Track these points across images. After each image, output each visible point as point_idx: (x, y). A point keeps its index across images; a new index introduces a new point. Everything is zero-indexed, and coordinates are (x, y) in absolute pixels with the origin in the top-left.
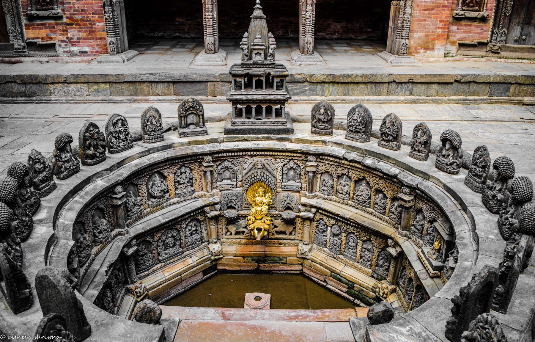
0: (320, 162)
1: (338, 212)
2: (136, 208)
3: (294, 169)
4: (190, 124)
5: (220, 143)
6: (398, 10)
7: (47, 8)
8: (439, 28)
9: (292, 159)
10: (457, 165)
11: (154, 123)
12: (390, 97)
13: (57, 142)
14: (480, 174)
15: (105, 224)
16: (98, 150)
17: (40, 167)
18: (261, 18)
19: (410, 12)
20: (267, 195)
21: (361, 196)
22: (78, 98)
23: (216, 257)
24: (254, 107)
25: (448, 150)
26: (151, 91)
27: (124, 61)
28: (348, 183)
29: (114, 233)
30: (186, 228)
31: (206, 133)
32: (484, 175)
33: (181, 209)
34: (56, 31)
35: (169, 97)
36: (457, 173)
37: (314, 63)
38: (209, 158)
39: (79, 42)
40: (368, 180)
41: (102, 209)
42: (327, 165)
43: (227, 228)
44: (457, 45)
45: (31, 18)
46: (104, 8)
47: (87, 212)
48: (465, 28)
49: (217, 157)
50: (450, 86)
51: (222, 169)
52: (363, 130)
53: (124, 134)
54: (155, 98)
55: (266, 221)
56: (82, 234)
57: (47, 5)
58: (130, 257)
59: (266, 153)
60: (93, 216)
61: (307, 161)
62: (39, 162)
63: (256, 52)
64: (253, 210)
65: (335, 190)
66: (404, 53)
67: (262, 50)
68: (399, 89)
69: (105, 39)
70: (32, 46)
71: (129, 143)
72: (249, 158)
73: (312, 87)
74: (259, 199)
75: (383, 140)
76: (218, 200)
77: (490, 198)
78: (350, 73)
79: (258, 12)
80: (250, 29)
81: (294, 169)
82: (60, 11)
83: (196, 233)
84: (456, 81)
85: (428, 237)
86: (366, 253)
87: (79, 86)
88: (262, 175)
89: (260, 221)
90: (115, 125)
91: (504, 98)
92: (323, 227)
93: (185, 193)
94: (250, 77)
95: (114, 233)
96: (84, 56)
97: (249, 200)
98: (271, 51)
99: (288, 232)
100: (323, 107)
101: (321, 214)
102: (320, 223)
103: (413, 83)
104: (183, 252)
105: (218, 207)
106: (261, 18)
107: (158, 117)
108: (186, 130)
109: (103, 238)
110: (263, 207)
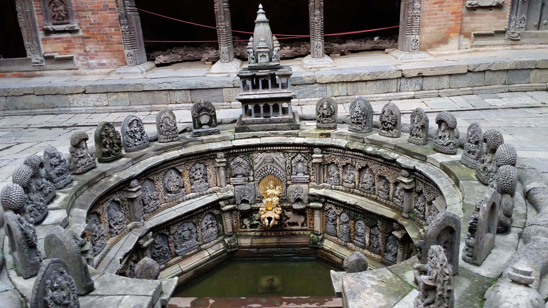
0: (326, 154)
1: (345, 200)
2: (152, 202)
3: (302, 162)
4: (204, 124)
5: (231, 140)
6: (407, 6)
7: (63, 22)
8: (451, 20)
9: (299, 152)
10: (454, 145)
11: (168, 124)
12: (400, 94)
13: (72, 140)
14: (474, 150)
15: (120, 216)
16: (114, 148)
17: (55, 161)
18: (264, 22)
19: (419, 7)
20: (277, 187)
21: (365, 183)
22: (98, 108)
23: (232, 250)
24: (261, 105)
25: (444, 131)
26: (169, 99)
27: (142, 73)
28: (353, 172)
29: (130, 225)
31: (218, 132)
32: (478, 151)
33: (197, 203)
34: (73, 45)
35: (187, 105)
36: (455, 154)
37: (324, 66)
39: (97, 55)
40: (370, 167)
41: (117, 203)
42: (332, 156)
43: (242, 222)
44: (472, 35)
45: (48, 32)
46: (120, 21)
47: (103, 204)
48: (480, 18)
49: (229, 154)
50: (463, 76)
52: (365, 121)
53: (139, 133)
54: (174, 106)
55: (277, 211)
56: (97, 225)
57: (63, 20)
58: (145, 249)
59: (274, 148)
60: (108, 208)
61: (313, 153)
62: (54, 157)
63: (261, 55)
64: (264, 201)
65: (341, 180)
66: (415, 49)
67: (266, 52)
68: (408, 83)
69: (123, 51)
70: (49, 59)
71: (144, 143)
73: (322, 88)
74: (269, 192)
75: (384, 129)
76: (231, 194)
77: (481, 170)
78: (358, 72)
79: (261, 17)
80: (254, 34)
81: (302, 162)
82: (76, 25)
83: (212, 226)
84: (469, 71)
85: (430, 217)
86: (374, 239)
87: (98, 96)
88: (272, 168)
89: (271, 212)
90: (130, 125)
91: (524, 85)
92: (332, 216)
94: (258, 77)
95: (130, 225)
96: (102, 68)
97: (262, 193)
98: (275, 53)
99: (300, 224)
100: (325, 103)
101: (330, 203)
102: (329, 213)
103: (423, 77)
104: (200, 246)
106: (264, 22)
107: (172, 118)
108: (200, 130)
109: (119, 230)
110: (274, 198)
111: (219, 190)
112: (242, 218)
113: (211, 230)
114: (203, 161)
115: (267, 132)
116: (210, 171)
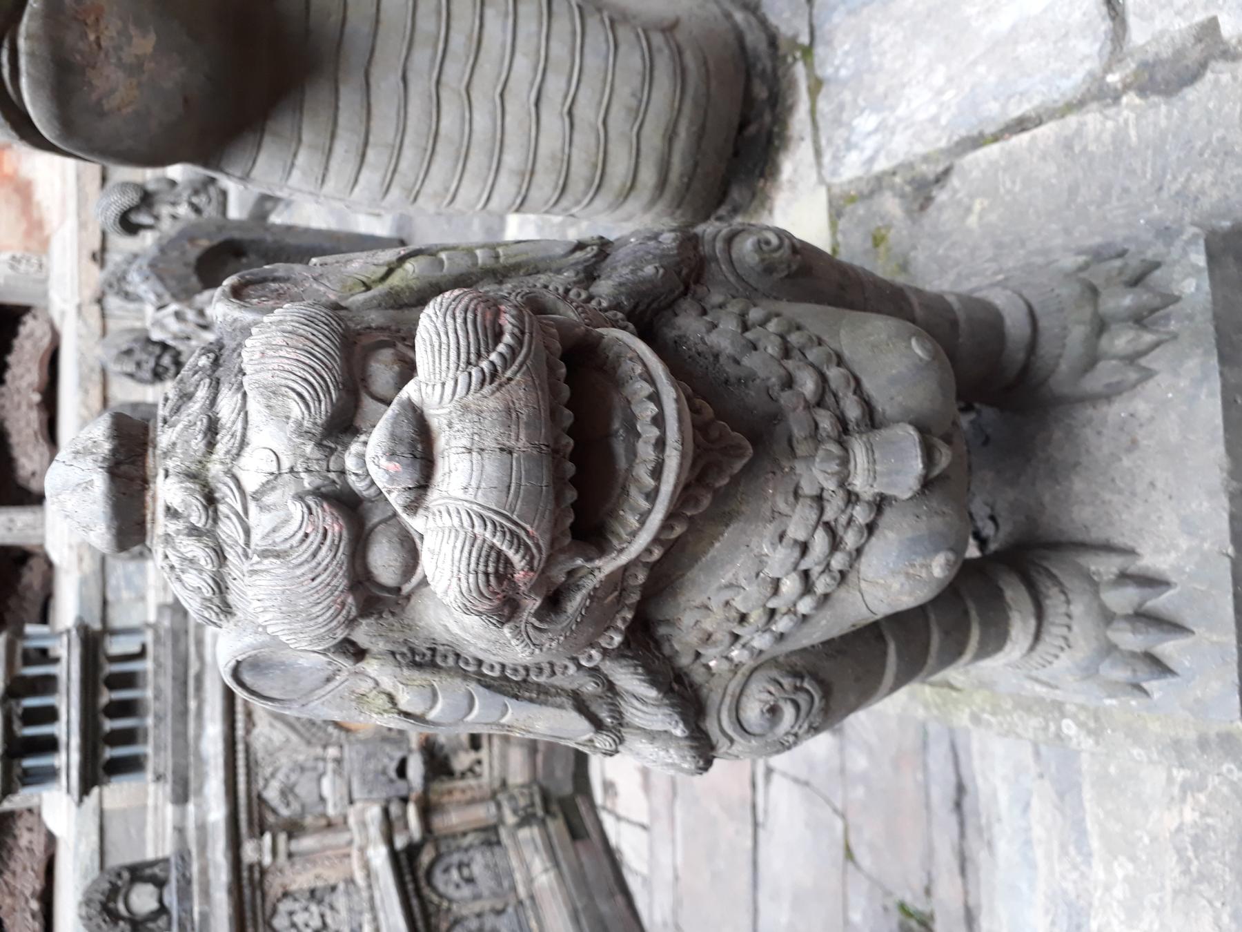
24: (109, 725)
30: (450, 901)
31: (183, 856)
36: (224, 194)
38: (249, 852)
51: (288, 805)
66: (41, 266)
72: (256, 731)
76: (375, 812)
93: (350, 910)
105: (395, 809)
111: (362, 850)
112: (450, 773)
113: (477, 869)
114: (269, 906)
115: (192, 704)
116: (301, 880)
